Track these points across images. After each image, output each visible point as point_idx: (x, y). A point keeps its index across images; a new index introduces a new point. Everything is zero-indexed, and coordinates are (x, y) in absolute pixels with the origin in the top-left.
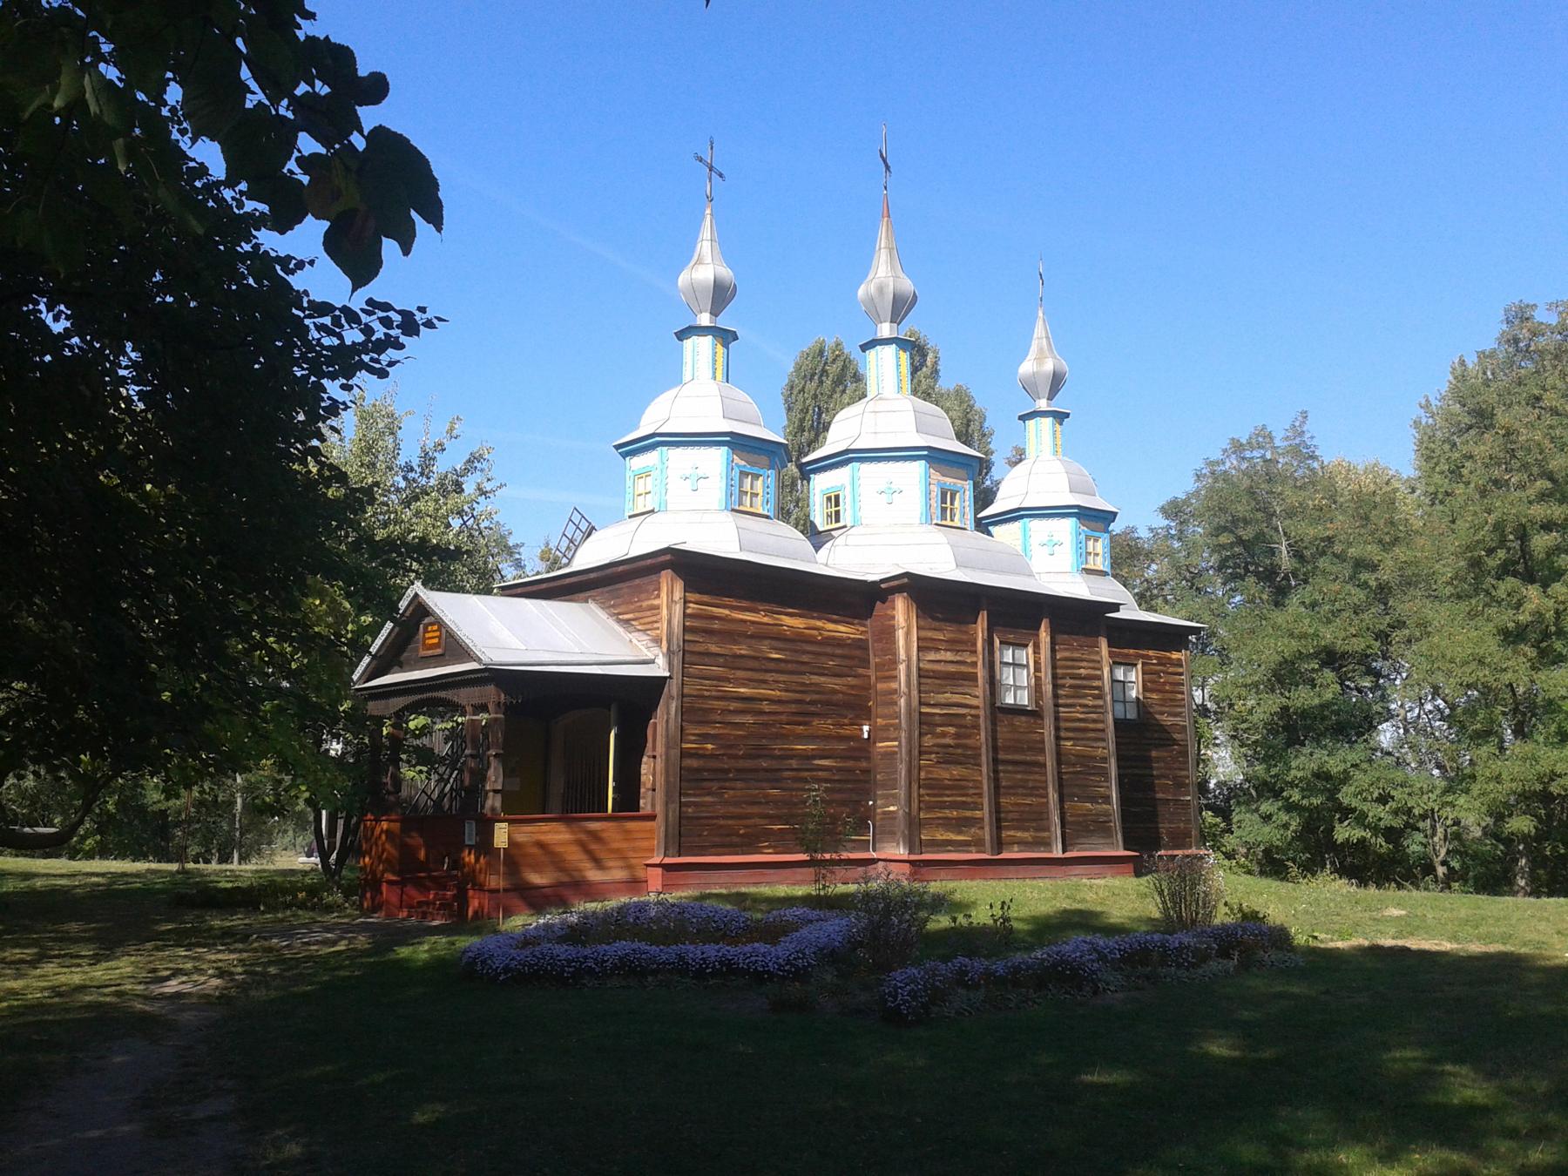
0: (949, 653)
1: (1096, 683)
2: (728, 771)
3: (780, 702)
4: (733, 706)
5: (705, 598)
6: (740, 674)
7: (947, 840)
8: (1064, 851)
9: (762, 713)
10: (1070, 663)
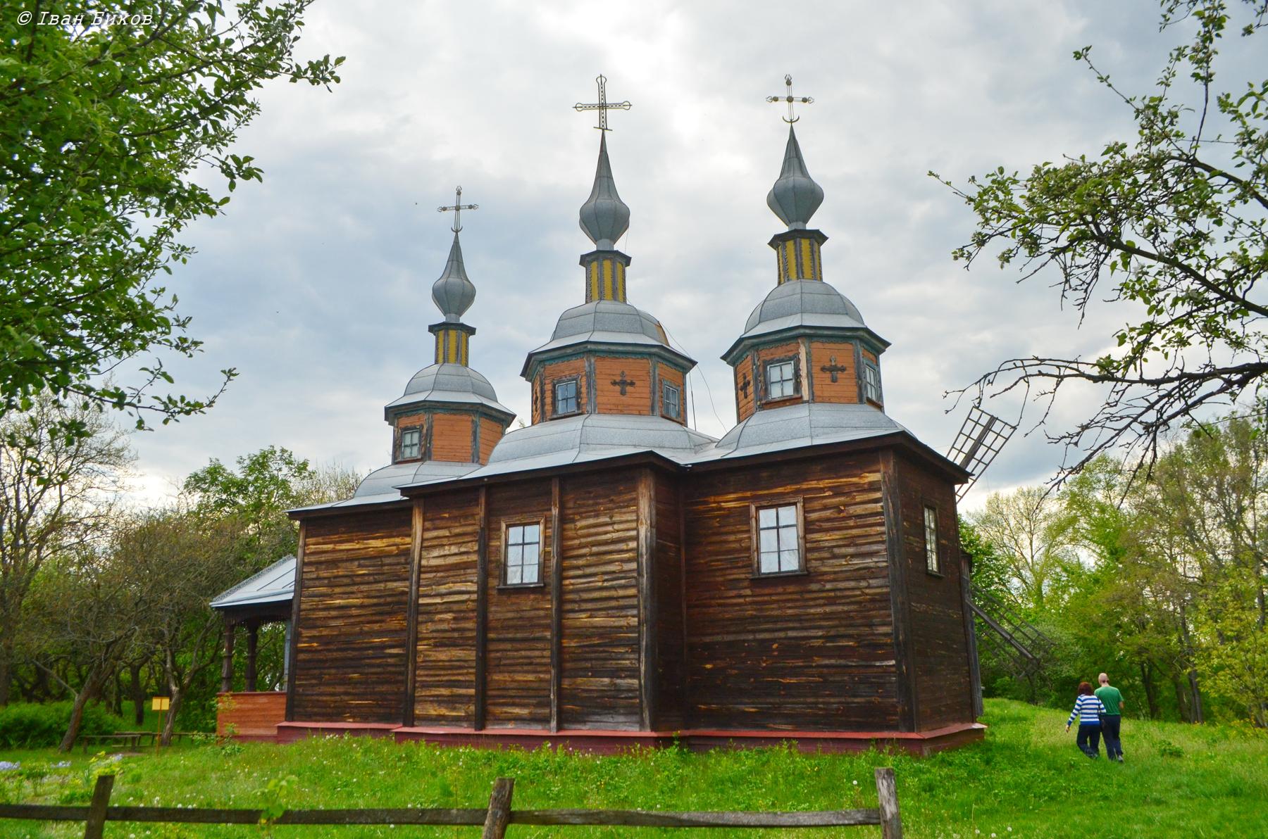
0: (453, 547)
1: (633, 545)
2: (326, 661)
3: (362, 606)
4: (333, 613)
5: (320, 539)
6: (337, 590)
7: (440, 715)
8: (559, 728)
9: (352, 616)
10: (592, 530)
